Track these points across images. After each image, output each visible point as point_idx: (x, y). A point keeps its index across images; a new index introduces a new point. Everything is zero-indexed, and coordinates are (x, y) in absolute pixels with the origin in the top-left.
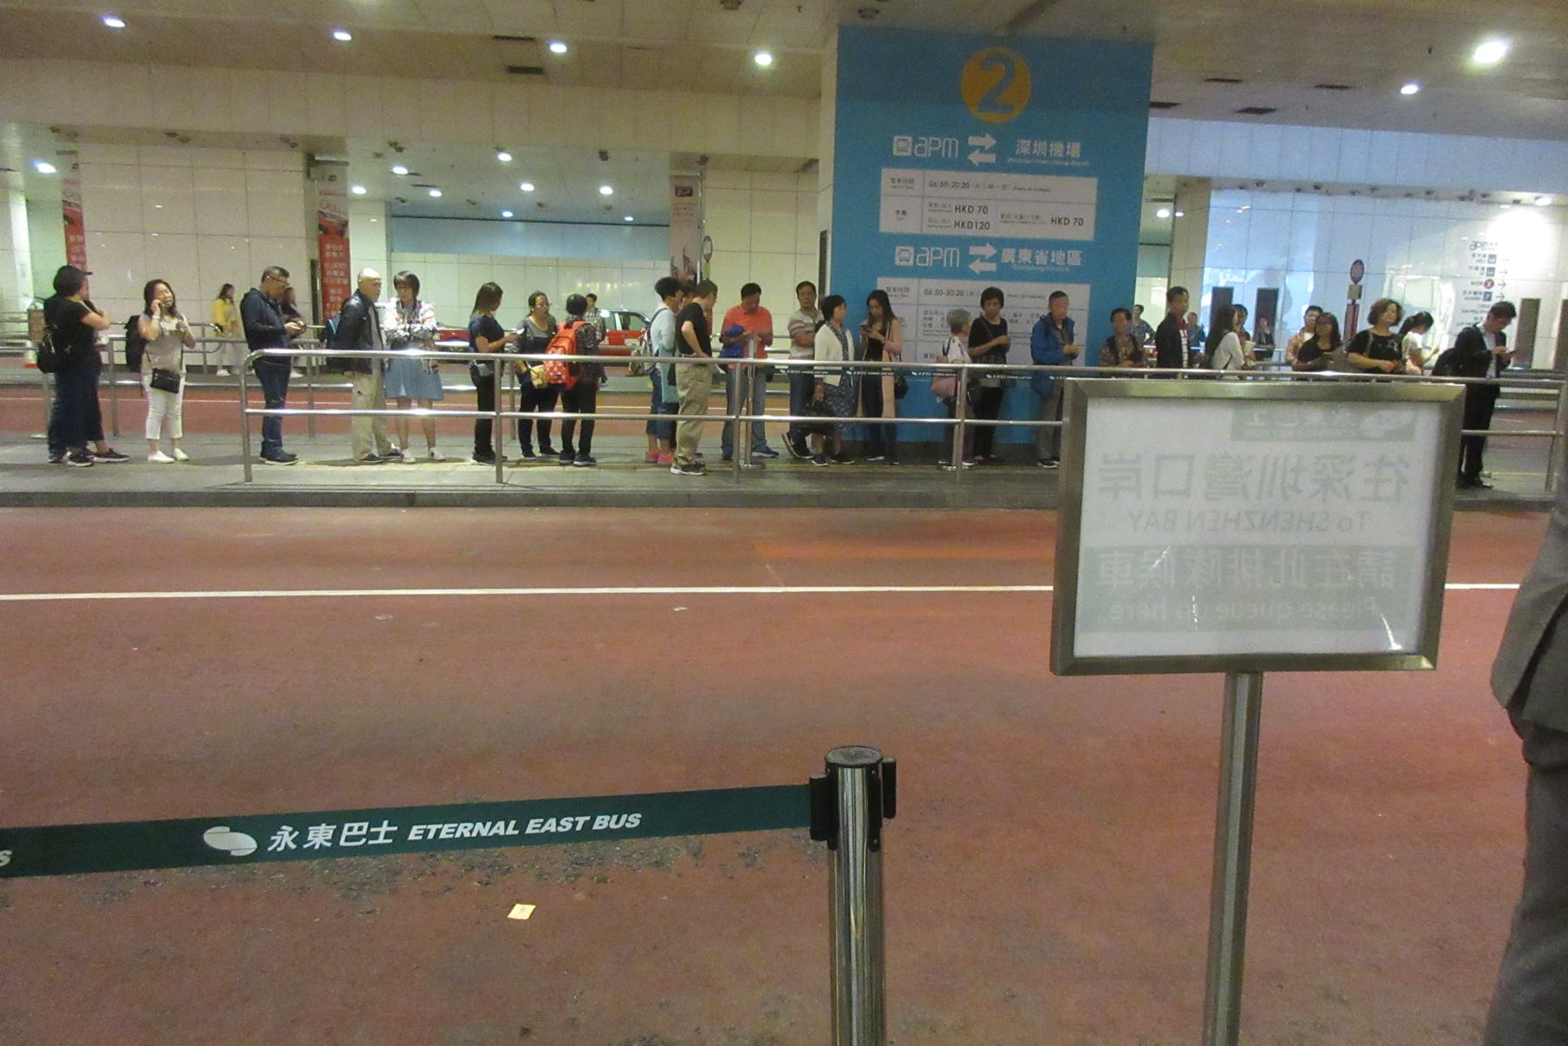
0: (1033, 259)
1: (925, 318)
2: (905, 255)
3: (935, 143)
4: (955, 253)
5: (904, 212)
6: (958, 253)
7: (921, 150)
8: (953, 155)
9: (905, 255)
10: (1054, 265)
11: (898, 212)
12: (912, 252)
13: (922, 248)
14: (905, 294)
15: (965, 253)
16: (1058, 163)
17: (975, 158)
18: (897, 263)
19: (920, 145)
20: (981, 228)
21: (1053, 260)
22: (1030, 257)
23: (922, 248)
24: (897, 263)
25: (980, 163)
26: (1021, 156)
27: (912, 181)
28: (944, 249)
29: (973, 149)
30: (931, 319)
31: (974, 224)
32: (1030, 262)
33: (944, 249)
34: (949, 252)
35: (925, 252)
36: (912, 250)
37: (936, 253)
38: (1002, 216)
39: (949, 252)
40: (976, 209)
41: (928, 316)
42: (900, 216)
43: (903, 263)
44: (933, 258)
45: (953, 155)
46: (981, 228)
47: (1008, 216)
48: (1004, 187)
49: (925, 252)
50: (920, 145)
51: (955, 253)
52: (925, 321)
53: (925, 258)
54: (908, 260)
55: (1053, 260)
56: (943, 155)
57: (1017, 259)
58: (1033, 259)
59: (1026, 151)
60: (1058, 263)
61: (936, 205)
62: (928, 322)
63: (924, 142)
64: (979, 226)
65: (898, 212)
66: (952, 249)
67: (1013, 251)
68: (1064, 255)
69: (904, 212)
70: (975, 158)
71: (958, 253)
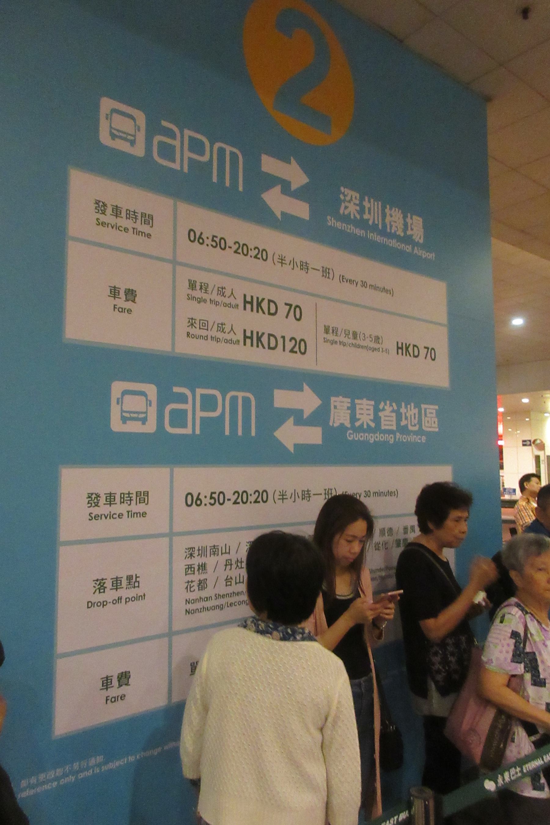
0: (377, 419)
1: (190, 567)
4: (246, 401)
5: (131, 294)
6: (253, 403)
10: (404, 430)
11: (114, 292)
14: (141, 508)
16: (393, 243)
18: (116, 425)
20: (292, 351)
21: (403, 423)
22: (372, 417)
23: (176, 389)
24: (116, 425)
26: (346, 219)
27: (148, 219)
30: (203, 567)
31: (280, 341)
32: (373, 425)
34: (234, 400)
35: (182, 399)
36: (151, 390)
38: (327, 331)
39: (234, 400)
40: (283, 310)
41: (196, 561)
42: (121, 302)
43: (134, 427)
46: (292, 351)
47: (335, 331)
48: (326, 272)
51: (246, 401)
52: (190, 578)
54: (144, 421)
55: (403, 423)
57: (353, 418)
58: (377, 419)
59: (352, 209)
60: (410, 428)
61: (204, 287)
62: (196, 577)
63: (172, 135)
64: (289, 345)
65: (114, 292)
66: (240, 395)
67: (347, 401)
68: (416, 411)
69: (131, 294)
71: (253, 403)
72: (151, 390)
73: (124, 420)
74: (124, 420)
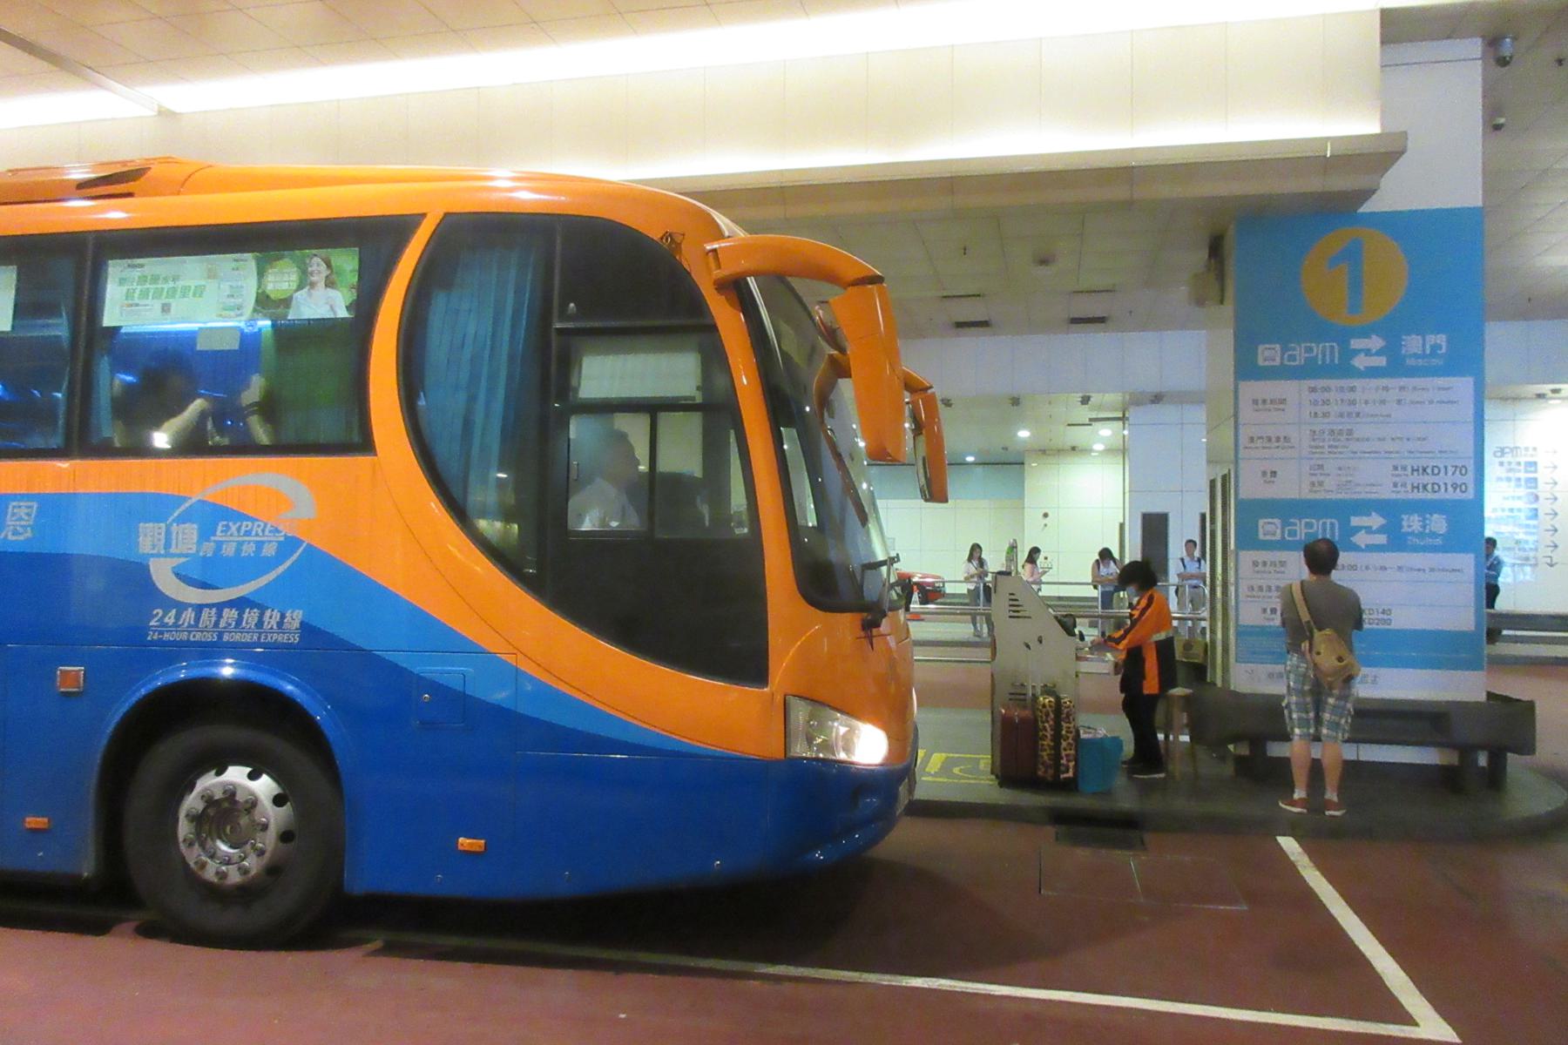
2: (1269, 528)
3: (1309, 350)
7: (1292, 358)
8: (1332, 360)
9: (1269, 528)
12: (1279, 526)
13: (1292, 520)
15: (1345, 524)
17: (1360, 362)
18: (1261, 537)
19: (1290, 353)
23: (1292, 520)
24: (1261, 537)
25: (1366, 367)
28: (1318, 521)
29: (1356, 352)
33: (1318, 521)
34: (1324, 524)
37: (1309, 525)
39: (1324, 524)
44: (1304, 531)
45: (1332, 360)
49: (1296, 525)
50: (1290, 353)
53: (1296, 531)
56: (1320, 363)
66: (1328, 521)
70: (1360, 362)
72: (1277, 521)
73: (1265, 535)
74: (1265, 535)
